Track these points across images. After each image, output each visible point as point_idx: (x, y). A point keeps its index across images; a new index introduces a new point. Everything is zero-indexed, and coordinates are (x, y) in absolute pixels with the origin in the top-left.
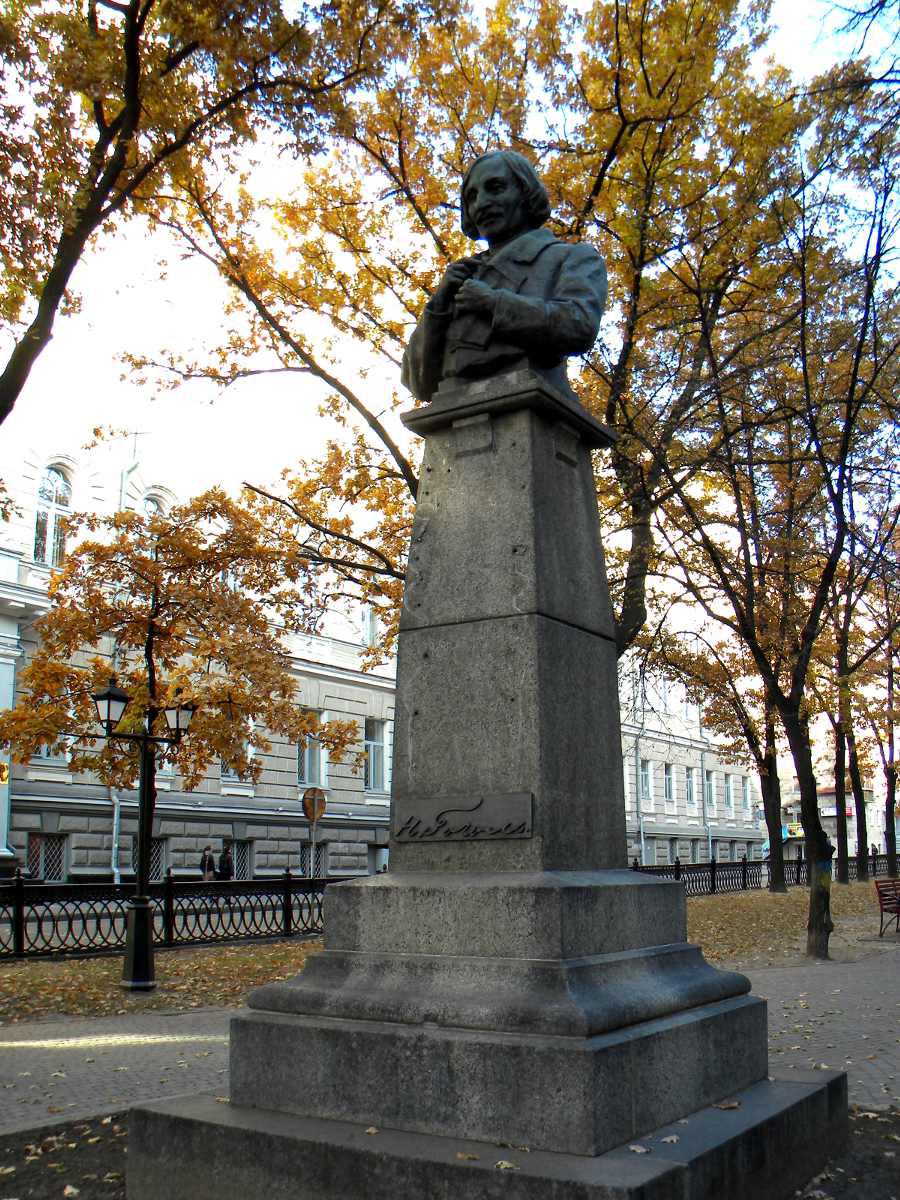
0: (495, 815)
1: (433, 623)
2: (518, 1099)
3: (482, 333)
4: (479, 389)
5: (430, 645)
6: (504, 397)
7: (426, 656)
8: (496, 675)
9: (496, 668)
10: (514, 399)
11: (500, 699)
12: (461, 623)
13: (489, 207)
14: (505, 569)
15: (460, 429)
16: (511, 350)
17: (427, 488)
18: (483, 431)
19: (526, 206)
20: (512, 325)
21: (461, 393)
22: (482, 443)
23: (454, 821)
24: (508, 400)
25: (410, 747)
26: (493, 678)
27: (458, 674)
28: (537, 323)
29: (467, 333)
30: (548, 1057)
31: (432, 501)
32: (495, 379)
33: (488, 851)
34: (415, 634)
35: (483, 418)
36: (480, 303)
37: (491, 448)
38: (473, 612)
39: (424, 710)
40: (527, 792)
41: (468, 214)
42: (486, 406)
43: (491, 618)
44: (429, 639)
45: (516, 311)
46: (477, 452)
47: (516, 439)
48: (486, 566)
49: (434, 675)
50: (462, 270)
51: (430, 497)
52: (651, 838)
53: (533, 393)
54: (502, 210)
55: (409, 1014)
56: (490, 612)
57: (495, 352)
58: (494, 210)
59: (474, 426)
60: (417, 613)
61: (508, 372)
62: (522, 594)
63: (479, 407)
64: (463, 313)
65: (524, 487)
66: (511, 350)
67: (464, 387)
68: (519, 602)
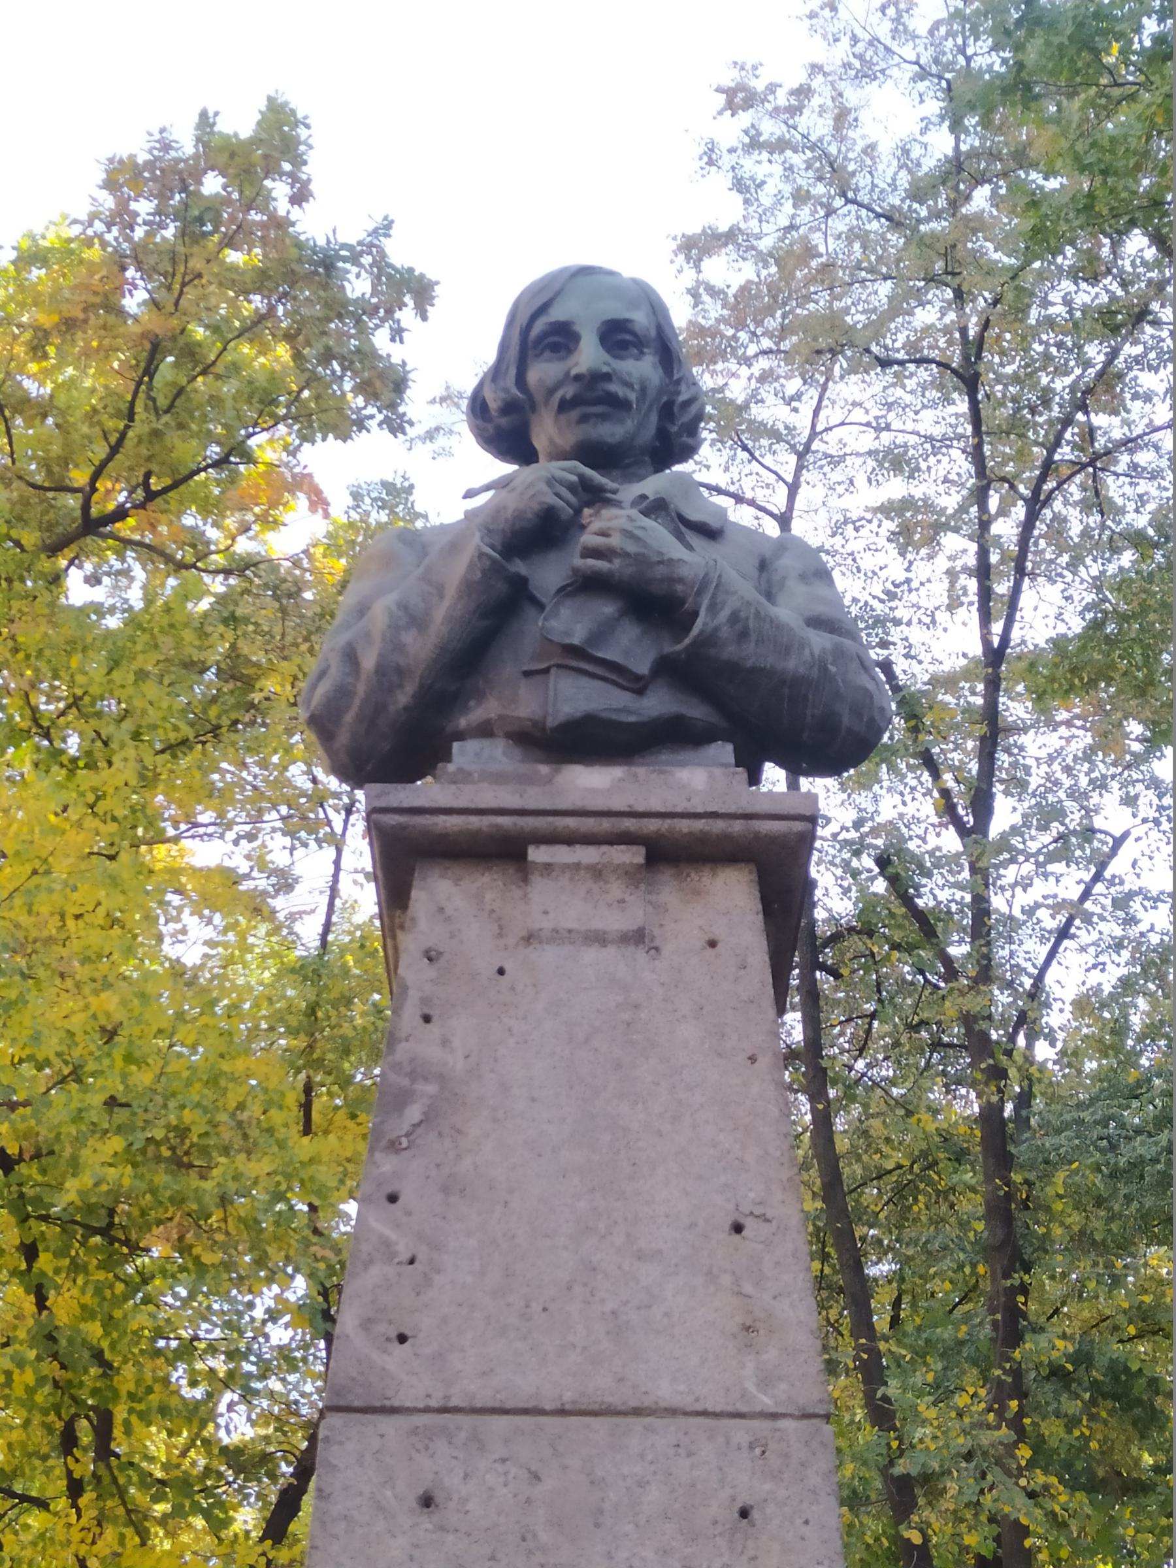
1: (454, 1402)
3: (633, 647)
4: (591, 783)
6: (714, 815)
7: (427, 1501)
10: (737, 826)
12: (562, 1412)
13: (607, 377)
14: (711, 1276)
15: (548, 867)
16: (697, 711)
17: (425, 1001)
18: (617, 889)
19: (668, 411)
20: (730, 652)
22: (616, 922)
24: (719, 826)
28: (792, 664)
29: (599, 635)
31: (445, 1042)
32: (641, 771)
34: (388, 1425)
36: (660, 571)
38: (602, 1386)
41: (521, 381)
42: (652, 826)
43: (673, 1412)
44: (440, 1445)
46: (599, 939)
47: (718, 932)
48: (640, 1256)
51: (434, 1029)
53: (798, 826)
54: (633, 397)
56: (665, 1392)
57: (658, 703)
58: (614, 388)
59: (597, 872)
60: (395, 1359)
61: (683, 765)
62: (771, 1355)
63: (629, 824)
64: (588, 585)
65: (752, 1059)
66: (697, 711)
67: (544, 769)
68: (766, 1382)
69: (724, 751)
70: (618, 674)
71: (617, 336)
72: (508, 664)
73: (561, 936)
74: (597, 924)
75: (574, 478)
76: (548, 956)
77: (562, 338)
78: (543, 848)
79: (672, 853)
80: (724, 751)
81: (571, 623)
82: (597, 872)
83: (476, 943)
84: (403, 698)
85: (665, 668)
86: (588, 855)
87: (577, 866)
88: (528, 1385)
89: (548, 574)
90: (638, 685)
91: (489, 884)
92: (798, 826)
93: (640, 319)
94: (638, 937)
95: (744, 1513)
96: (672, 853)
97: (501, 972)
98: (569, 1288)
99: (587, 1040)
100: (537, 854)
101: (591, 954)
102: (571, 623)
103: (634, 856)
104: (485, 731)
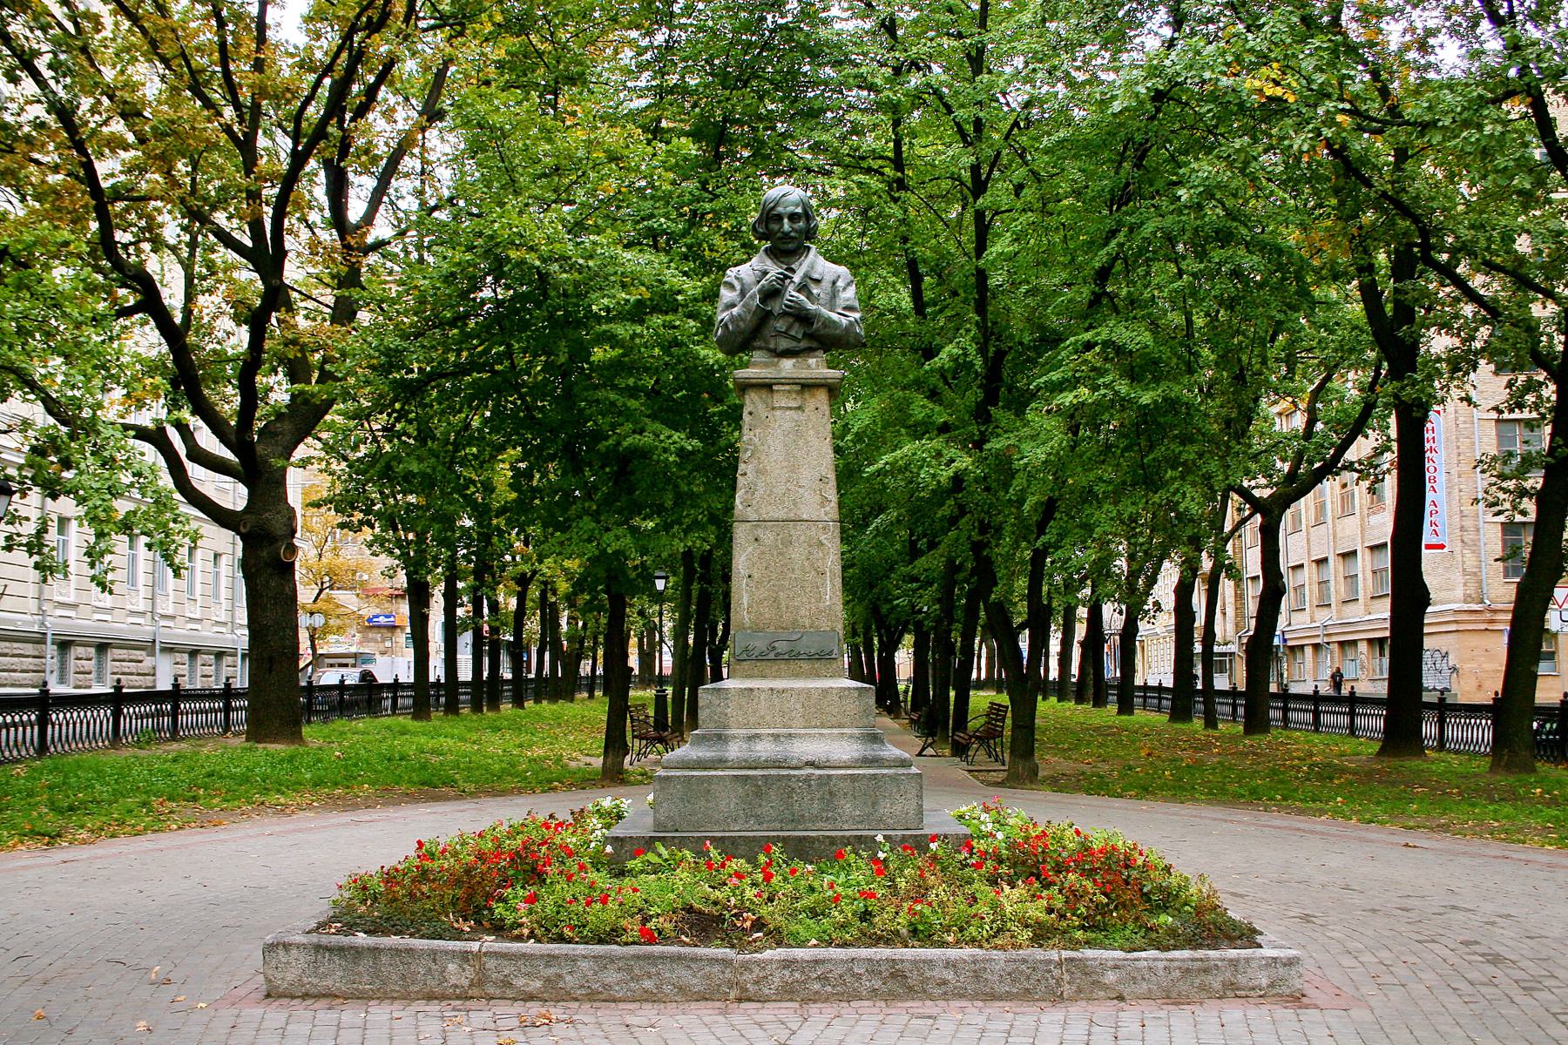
0: (809, 645)
2: (874, 804)
3: (797, 331)
4: (788, 366)
5: (759, 532)
16: (815, 345)
21: (776, 365)
22: (793, 404)
23: (782, 647)
25: (745, 601)
29: (790, 327)
30: (893, 778)
33: (805, 666)
35: (798, 388)
37: (799, 408)
39: (756, 575)
40: (833, 630)
45: (829, 323)
49: (763, 553)
52: (169, 649)
55: (794, 762)
57: (804, 344)
64: (785, 314)
69: (820, 353)
70: (794, 338)
71: (793, 217)
72: (767, 332)
76: (778, 413)
77: (780, 218)
81: (781, 325)
83: (762, 410)
84: (740, 339)
85: (805, 335)
88: (776, 516)
89: (776, 306)
90: (799, 341)
91: (764, 394)
93: (799, 210)
94: (799, 408)
96: (807, 387)
102: (781, 325)
103: (798, 388)
104: (760, 348)
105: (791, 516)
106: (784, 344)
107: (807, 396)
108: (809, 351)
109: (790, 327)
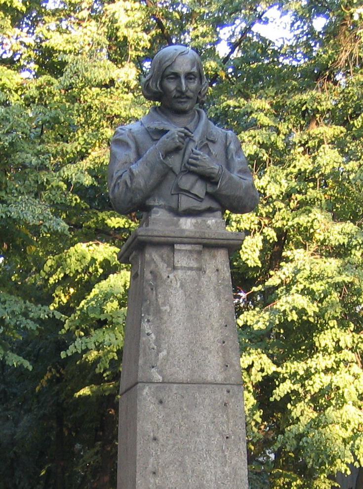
3: (199, 189)
4: (187, 224)
8: (216, 420)
9: (215, 417)
11: (218, 436)
12: (188, 383)
16: (214, 205)
22: (194, 264)
26: (213, 422)
27: (187, 417)
35: (198, 248)
39: (161, 440)
42: (205, 241)
46: (191, 269)
48: (203, 349)
50: (182, 137)
56: (210, 378)
63: (200, 240)
73: (182, 268)
74: (191, 265)
75: (183, 135)
78: (178, 245)
79: (208, 245)
80: (219, 213)
82: (190, 251)
85: (207, 193)
86: (188, 247)
87: (186, 250)
91: (165, 251)
92: (240, 241)
95: (225, 405)
96: (208, 245)
97: (168, 277)
98: (188, 356)
99: (189, 295)
100: (177, 247)
101: (189, 273)
105: (196, 377)
106: (186, 202)
107: (206, 256)
108: (210, 210)
109: (192, 187)
